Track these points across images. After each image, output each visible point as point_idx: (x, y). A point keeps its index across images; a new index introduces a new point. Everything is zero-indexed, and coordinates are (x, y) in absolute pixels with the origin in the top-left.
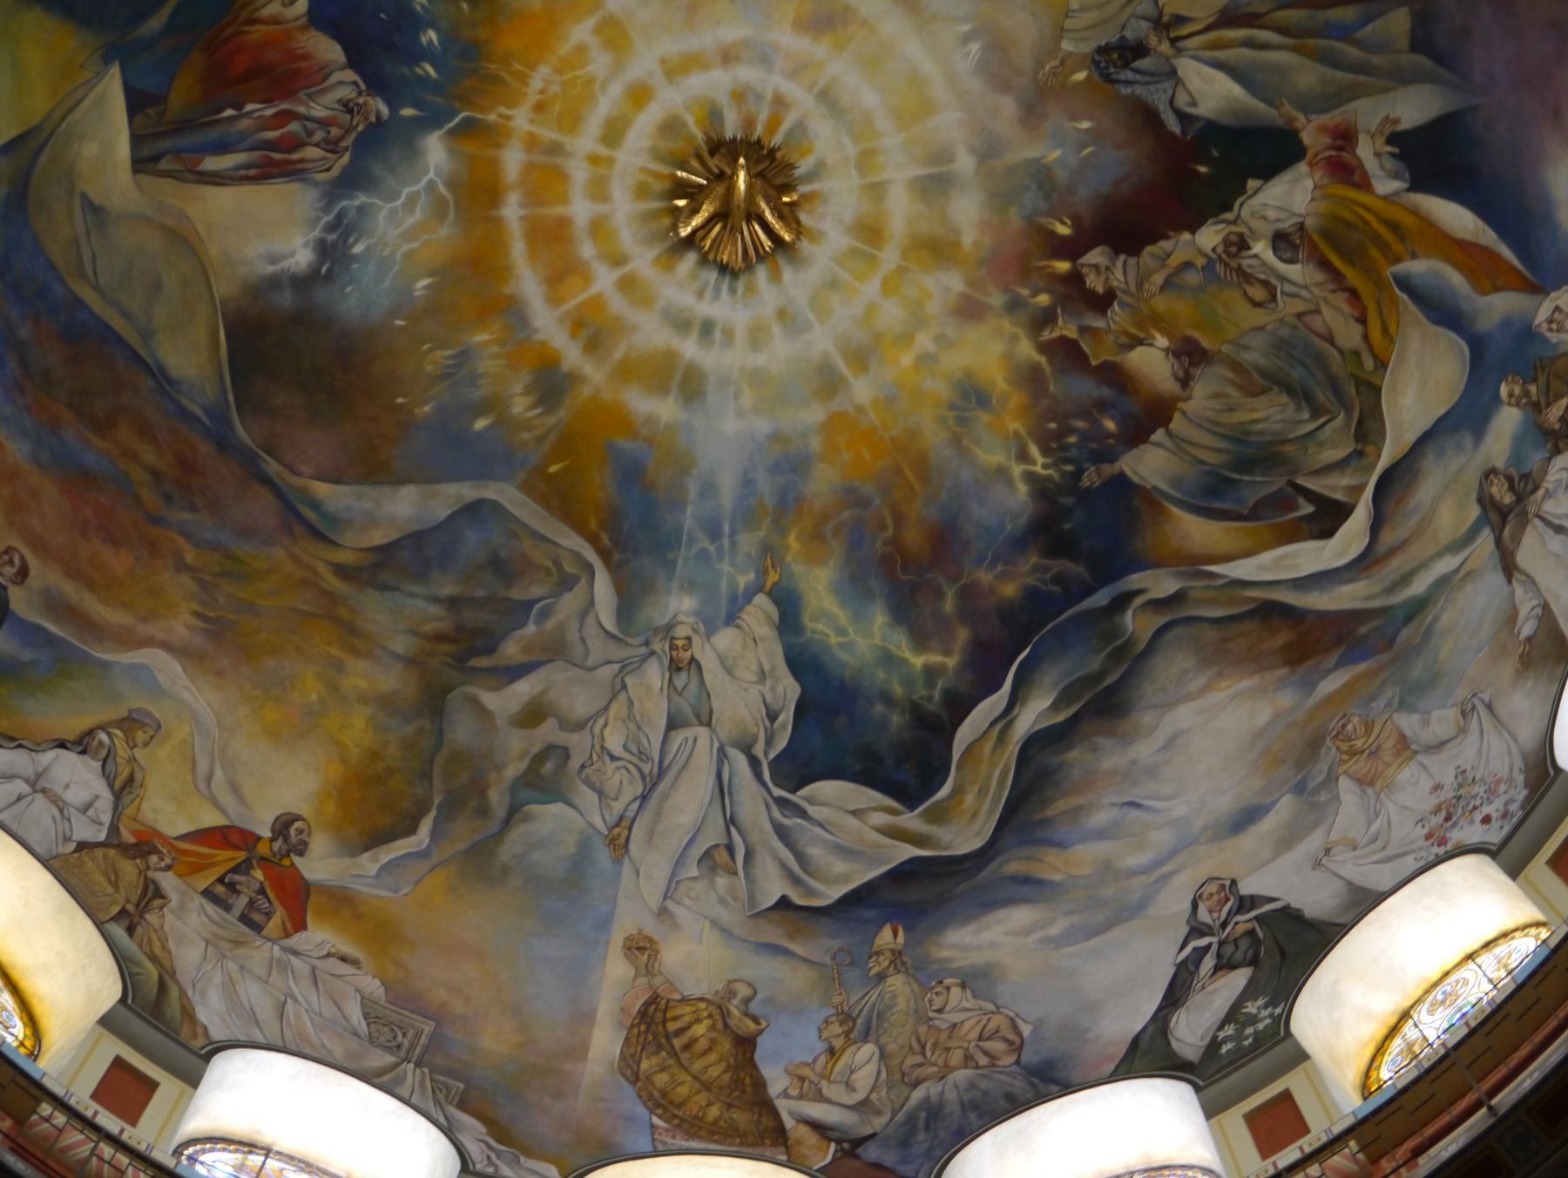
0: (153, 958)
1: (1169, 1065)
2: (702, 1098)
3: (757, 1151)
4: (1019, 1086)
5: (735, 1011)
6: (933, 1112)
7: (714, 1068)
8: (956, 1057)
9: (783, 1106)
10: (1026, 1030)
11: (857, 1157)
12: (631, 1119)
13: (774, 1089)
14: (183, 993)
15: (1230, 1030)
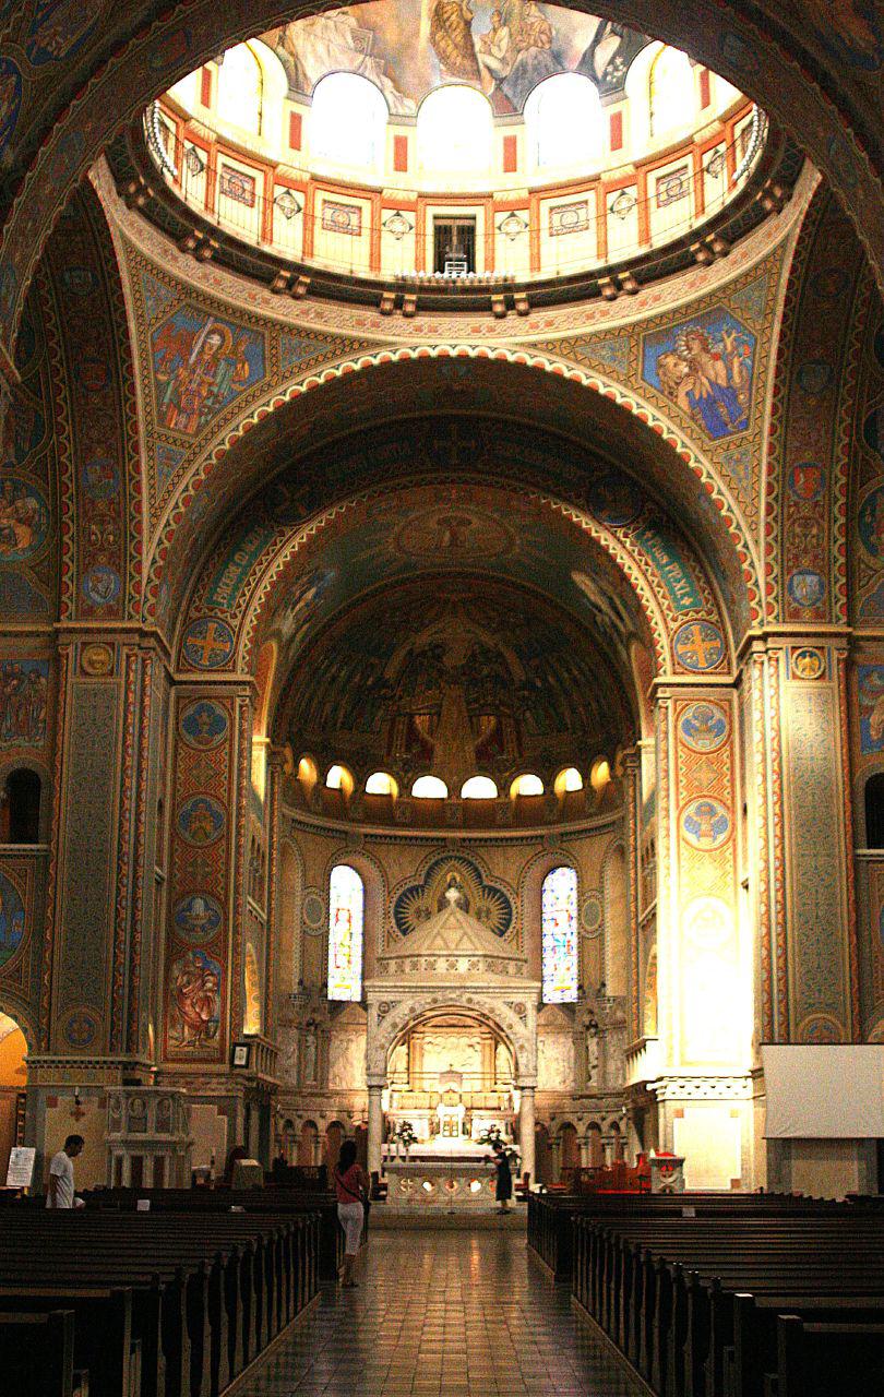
0: (292, 54)
1: (594, 78)
2: (455, 53)
3: (470, 82)
4: (549, 61)
5: (465, 8)
6: (523, 65)
7: (458, 37)
8: (532, 42)
9: (479, 55)
10: (554, 32)
11: (500, 89)
12: (433, 66)
13: (477, 48)
14: (302, 66)
15: (610, 69)
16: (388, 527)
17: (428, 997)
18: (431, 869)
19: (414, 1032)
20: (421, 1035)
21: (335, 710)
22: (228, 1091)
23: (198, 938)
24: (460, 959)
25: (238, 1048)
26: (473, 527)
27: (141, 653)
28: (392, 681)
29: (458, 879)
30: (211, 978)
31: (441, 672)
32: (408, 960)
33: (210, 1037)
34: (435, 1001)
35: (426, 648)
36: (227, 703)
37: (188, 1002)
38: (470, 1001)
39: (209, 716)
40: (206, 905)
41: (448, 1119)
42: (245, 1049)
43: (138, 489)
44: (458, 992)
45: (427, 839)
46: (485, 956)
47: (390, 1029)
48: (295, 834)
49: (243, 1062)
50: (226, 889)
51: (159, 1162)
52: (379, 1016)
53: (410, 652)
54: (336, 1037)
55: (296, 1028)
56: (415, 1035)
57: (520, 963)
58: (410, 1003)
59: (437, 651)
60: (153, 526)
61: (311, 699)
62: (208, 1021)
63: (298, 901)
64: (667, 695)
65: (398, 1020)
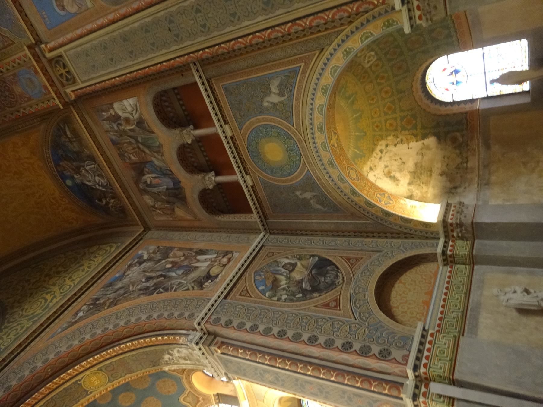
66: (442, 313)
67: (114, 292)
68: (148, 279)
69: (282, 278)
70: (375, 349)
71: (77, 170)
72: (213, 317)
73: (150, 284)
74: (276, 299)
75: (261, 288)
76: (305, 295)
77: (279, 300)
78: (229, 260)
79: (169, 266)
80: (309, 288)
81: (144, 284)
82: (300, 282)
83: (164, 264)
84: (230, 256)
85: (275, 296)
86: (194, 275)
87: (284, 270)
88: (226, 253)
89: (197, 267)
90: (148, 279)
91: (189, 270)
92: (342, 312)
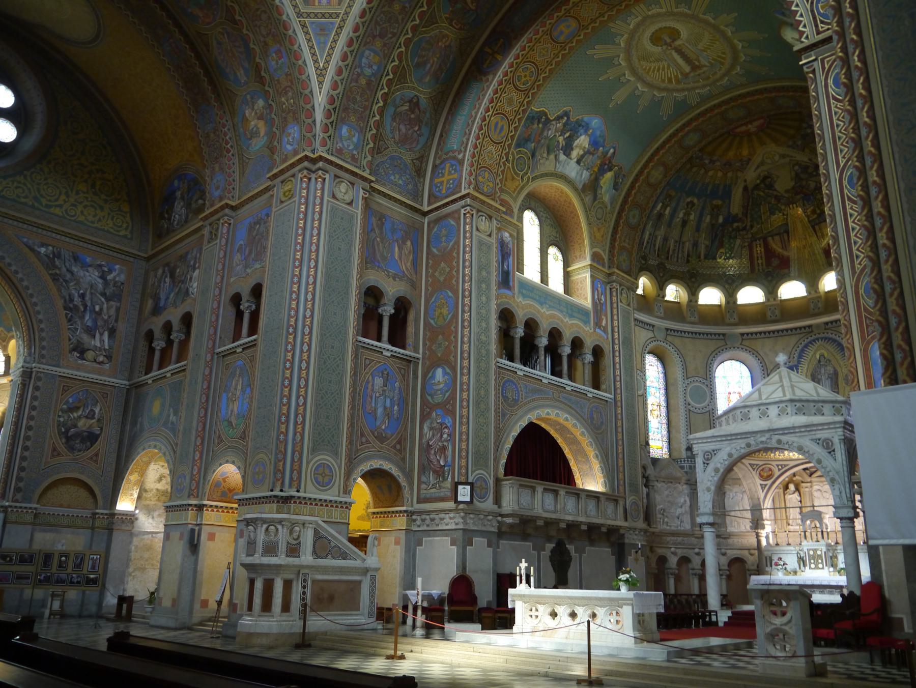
16: (609, 62)
17: (742, 443)
18: (802, 351)
19: (802, 482)
20: (809, 485)
21: (695, 245)
22: (457, 524)
23: (439, 398)
24: (770, 407)
25: (460, 487)
26: (684, 34)
27: (313, 176)
28: (740, 216)
29: (826, 355)
30: (446, 430)
31: (778, 199)
32: (731, 414)
33: (445, 479)
34: (748, 445)
35: (758, 182)
36: (456, 215)
37: (433, 452)
38: (779, 442)
39: (445, 230)
40: (445, 373)
41: (811, 553)
42: (468, 487)
43: (297, 56)
44: (767, 435)
45: (796, 329)
46: (791, 401)
47: (713, 474)
48: (669, 338)
49: (468, 499)
50: (455, 357)
51: (288, 585)
52: (704, 463)
53: (745, 189)
54: (731, 491)
55: (686, 484)
56: (804, 485)
57: (838, 405)
58: (728, 449)
59: (768, 181)
60: (321, 83)
61: (665, 239)
62: (444, 466)
63: (681, 389)
64: (813, 58)
65: (719, 465)
66: (54, 514)
67: (67, 270)
68: (82, 296)
69: (80, 413)
70: (21, 485)
71: (182, 198)
72: (42, 375)
73: (77, 300)
74: (60, 414)
75: (71, 400)
76: (63, 433)
77: (59, 416)
78: (100, 363)
79: (97, 308)
80: (70, 434)
81: (76, 295)
82: (75, 426)
83: (99, 302)
84: (106, 360)
85: (63, 413)
86: (85, 338)
87: (87, 411)
88: (109, 357)
89: (94, 337)
90: (82, 296)
91: (91, 332)
92: (49, 460)
